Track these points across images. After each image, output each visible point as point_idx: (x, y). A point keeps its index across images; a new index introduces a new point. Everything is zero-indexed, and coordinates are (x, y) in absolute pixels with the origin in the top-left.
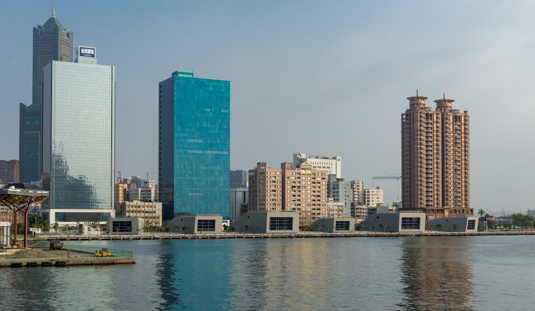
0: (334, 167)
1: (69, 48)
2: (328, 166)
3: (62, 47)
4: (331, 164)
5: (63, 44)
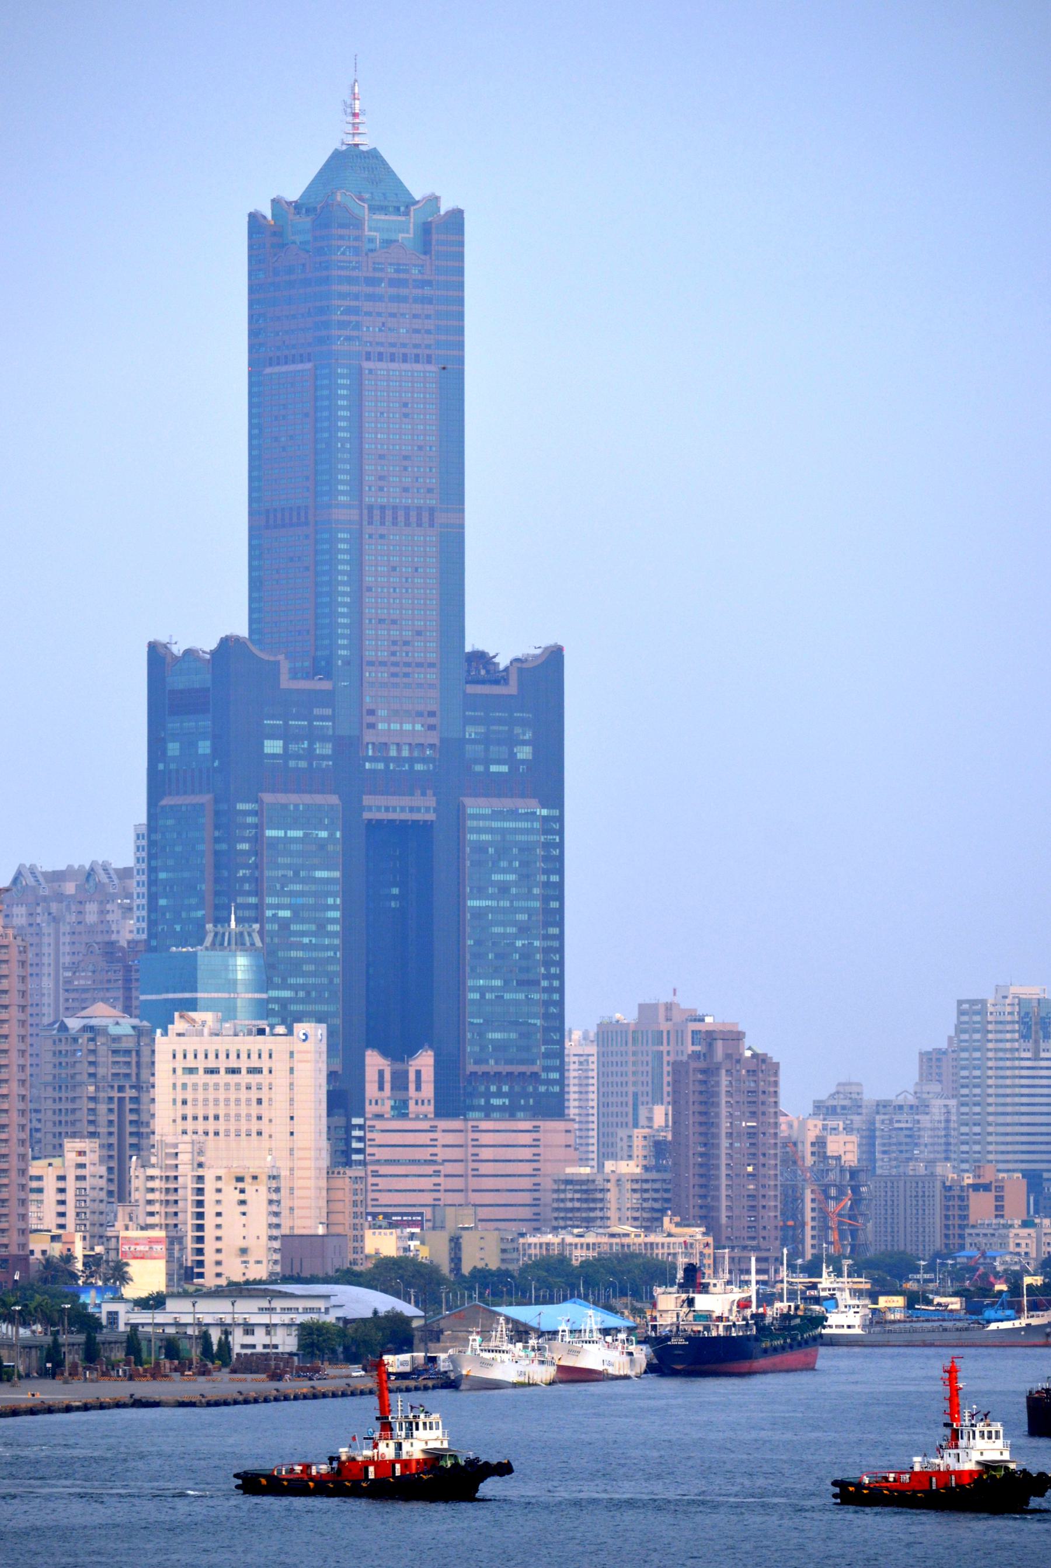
0: (280, 1065)
1: (429, 309)
2: (255, 1063)
3: (368, 314)
4: (265, 1056)
5: (371, 297)
